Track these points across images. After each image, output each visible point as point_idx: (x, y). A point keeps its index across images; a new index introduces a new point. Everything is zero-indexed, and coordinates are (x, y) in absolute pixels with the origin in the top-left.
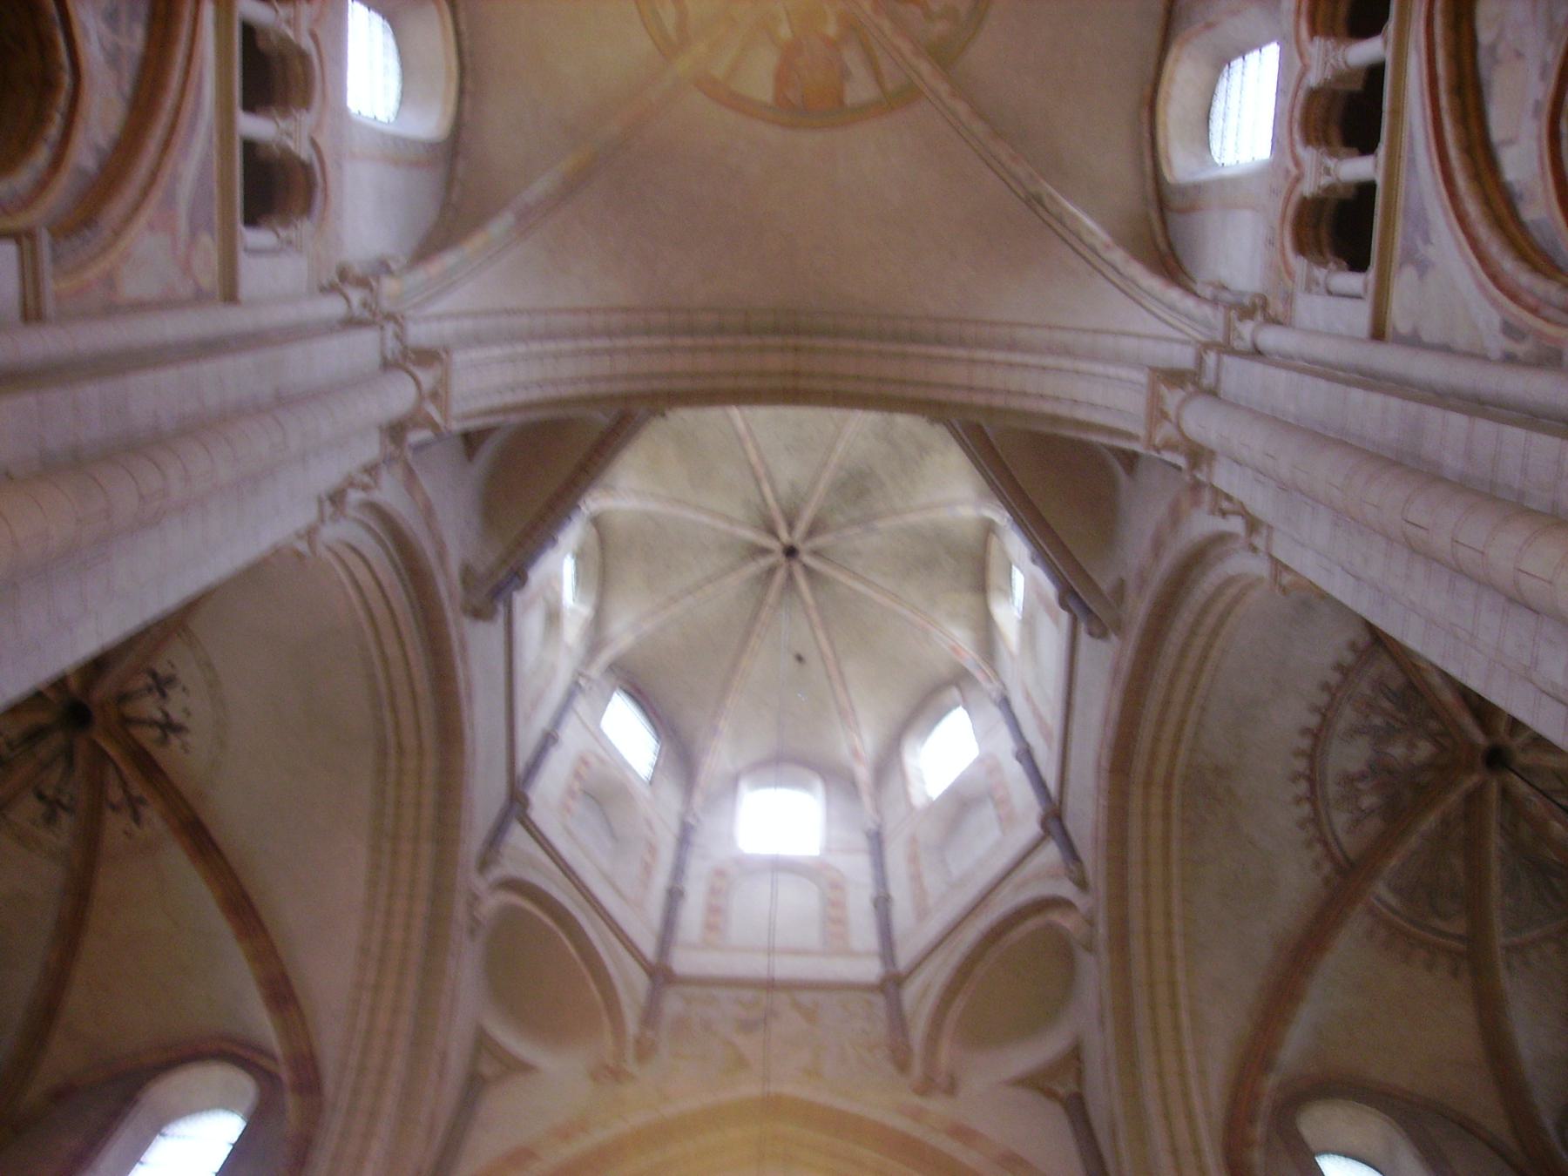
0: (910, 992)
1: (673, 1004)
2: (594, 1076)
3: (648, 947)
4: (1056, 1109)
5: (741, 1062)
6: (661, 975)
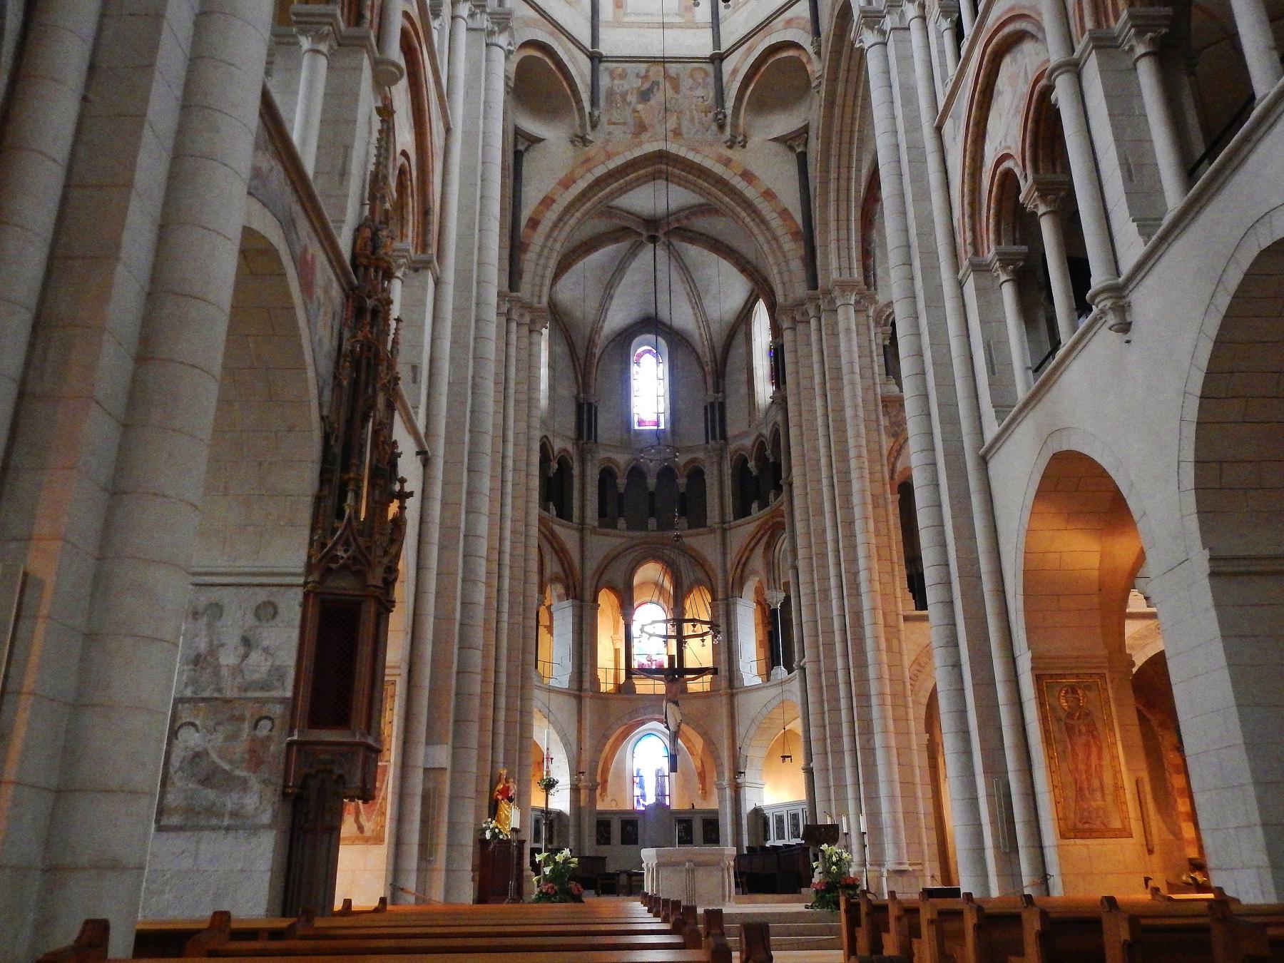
0: (728, 65)
1: (604, 81)
2: (572, 142)
3: (586, 41)
4: (792, 157)
5: (641, 128)
6: (596, 58)
